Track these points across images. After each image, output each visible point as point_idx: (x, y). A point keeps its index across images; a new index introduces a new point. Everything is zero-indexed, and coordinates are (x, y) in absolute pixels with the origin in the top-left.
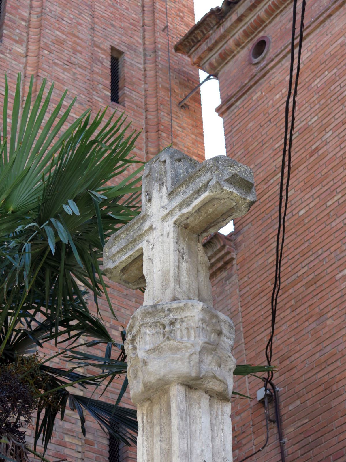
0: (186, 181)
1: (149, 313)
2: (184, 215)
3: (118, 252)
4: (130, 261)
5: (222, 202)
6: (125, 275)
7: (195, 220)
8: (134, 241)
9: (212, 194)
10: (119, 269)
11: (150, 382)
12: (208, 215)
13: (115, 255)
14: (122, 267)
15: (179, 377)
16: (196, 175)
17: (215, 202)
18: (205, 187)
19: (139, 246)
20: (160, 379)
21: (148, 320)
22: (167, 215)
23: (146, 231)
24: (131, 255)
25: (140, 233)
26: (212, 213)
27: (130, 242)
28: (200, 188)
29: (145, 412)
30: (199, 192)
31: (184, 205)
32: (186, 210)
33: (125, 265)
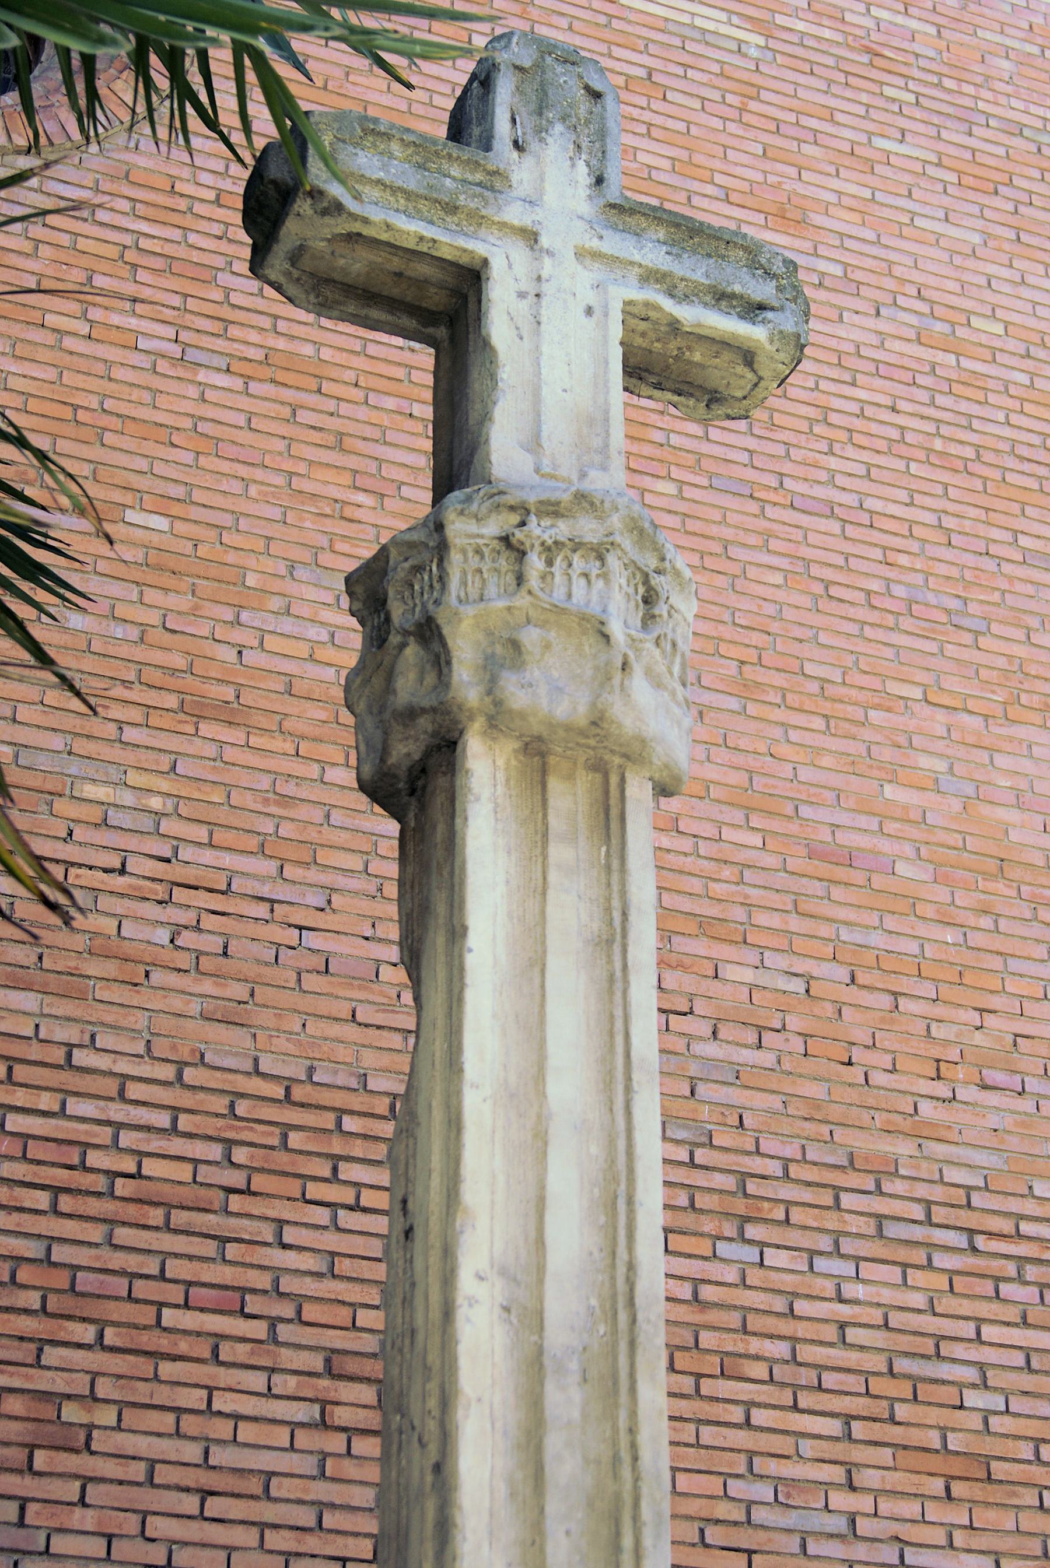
0: (678, 226)
1: (642, 531)
2: (658, 308)
3: (379, 182)
4: (411, 245)
5: (740, 369)
6: (323, 244)
7: (643, 335)
8: (452, 209)
9: (768, 347)
10: (357, 227)
11: (620, 726)
12: (676, 358)
13: (362, 179)
14: (366, 231)
15: (666, 766)
16: (714, 243)
17: (727, 356)
18: (754, 310)
19: (479, 248)
20: (643, 741)
21: (626, 542)
22: (597, 255)
23: (503, 225)
24: (434, 241)
25: (484, 212)
26: (689, 362)
27: (436, 201)
28: (733, 296)
29: (501, 762)
30: (720, 297)
31: (657, 281)
32: (668, 304)
33: (384, 237)
